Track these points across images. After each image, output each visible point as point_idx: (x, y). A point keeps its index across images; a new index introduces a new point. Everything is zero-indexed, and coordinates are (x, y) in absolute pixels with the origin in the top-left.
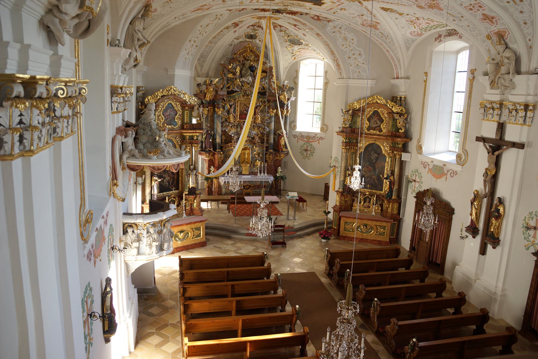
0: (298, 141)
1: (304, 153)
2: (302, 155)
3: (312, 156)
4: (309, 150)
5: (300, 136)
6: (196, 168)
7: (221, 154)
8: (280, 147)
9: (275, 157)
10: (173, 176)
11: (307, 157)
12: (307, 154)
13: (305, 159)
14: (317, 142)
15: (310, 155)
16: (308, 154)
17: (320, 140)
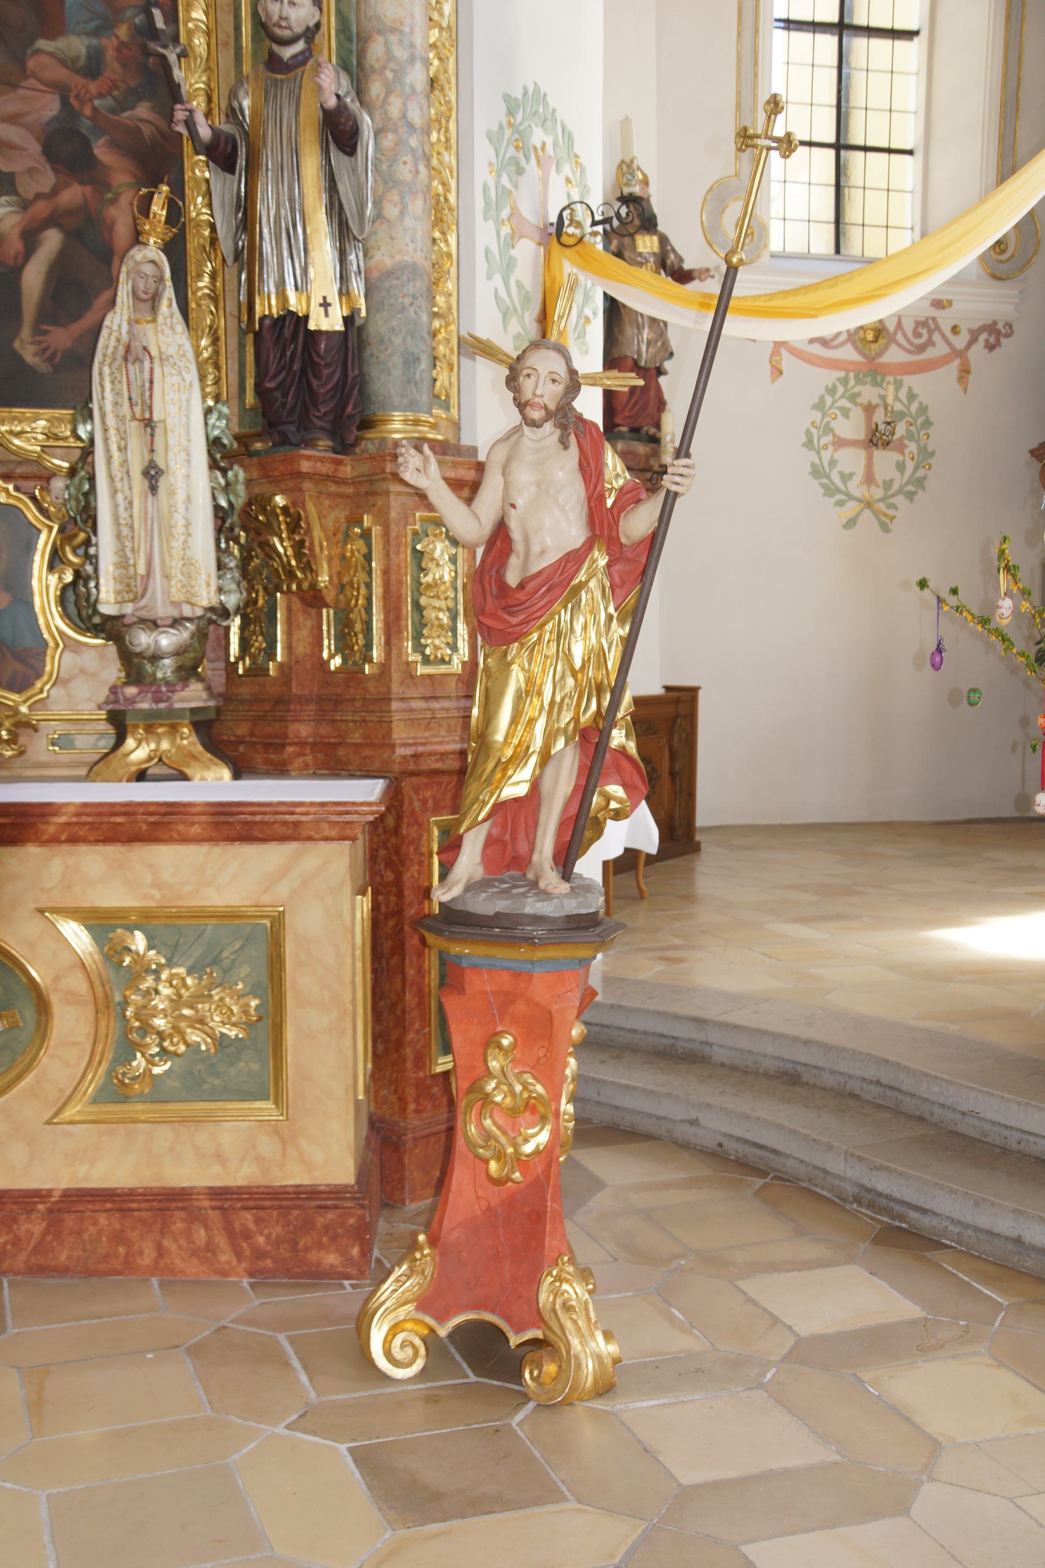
6: (376, 50)
10: (73, 194)
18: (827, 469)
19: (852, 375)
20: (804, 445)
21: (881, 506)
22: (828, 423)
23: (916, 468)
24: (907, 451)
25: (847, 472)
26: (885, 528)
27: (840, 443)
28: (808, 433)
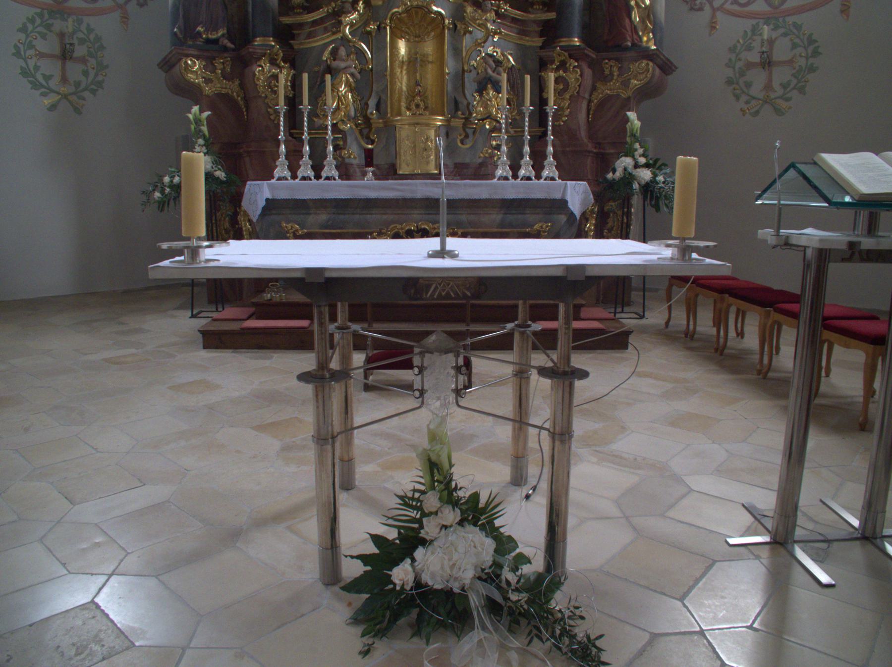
1: (748, 85)
2: (737, 98)
3: (802, 90)
4: (780, 63)
7: (273, 62)
8: (627, 21)
9: (594, 89)
12: (768, 87)
15: (784, 86)
16: (776, 84)
18: (33, 72)
19: (46, 11)
20: (14, 54)
21: (73, 98)
22: (30, 42)
23: (96, 75)
24: (89, 64)
25: (48, 74)
26: (77, 110)
27: (41, 55)
28: (16, 46)
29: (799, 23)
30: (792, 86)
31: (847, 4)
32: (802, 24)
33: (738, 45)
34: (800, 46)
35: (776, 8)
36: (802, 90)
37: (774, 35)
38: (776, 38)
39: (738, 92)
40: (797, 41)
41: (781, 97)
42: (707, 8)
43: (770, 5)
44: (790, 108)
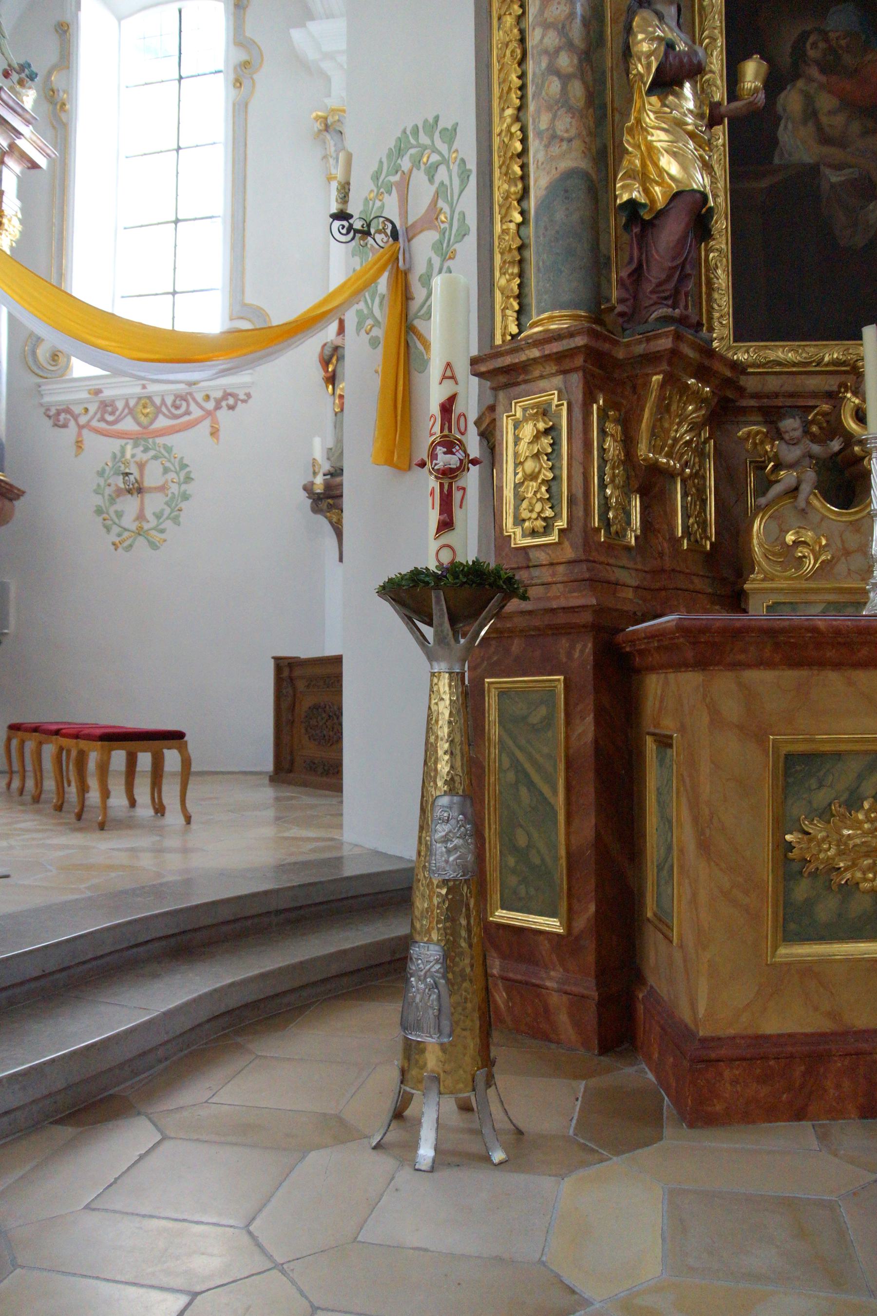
0: (79, 444)
1: (119, 514)
2: (108, 529)
3: (176, 520)
5: (93, 408)
11: (140, 532)
12: (141, 516)
13: (131, 546)
14: (205, 427)
15: (158, 516)
16: (149, 514)
17: (223, 415)
29: (169, 445)
30: (165, 516)
31: (217, 426)
32: (172, 446)
33: (107, 468)
34: (172, 471)
35: (145, 428)
36: (176, 520)
37: (145, 457)
38: (147, 462)
39: (109, 522)
40: (168, 465)
41: (154, 529)
42: (72, 424)
43: (139, 424)
44: (165, 541)
